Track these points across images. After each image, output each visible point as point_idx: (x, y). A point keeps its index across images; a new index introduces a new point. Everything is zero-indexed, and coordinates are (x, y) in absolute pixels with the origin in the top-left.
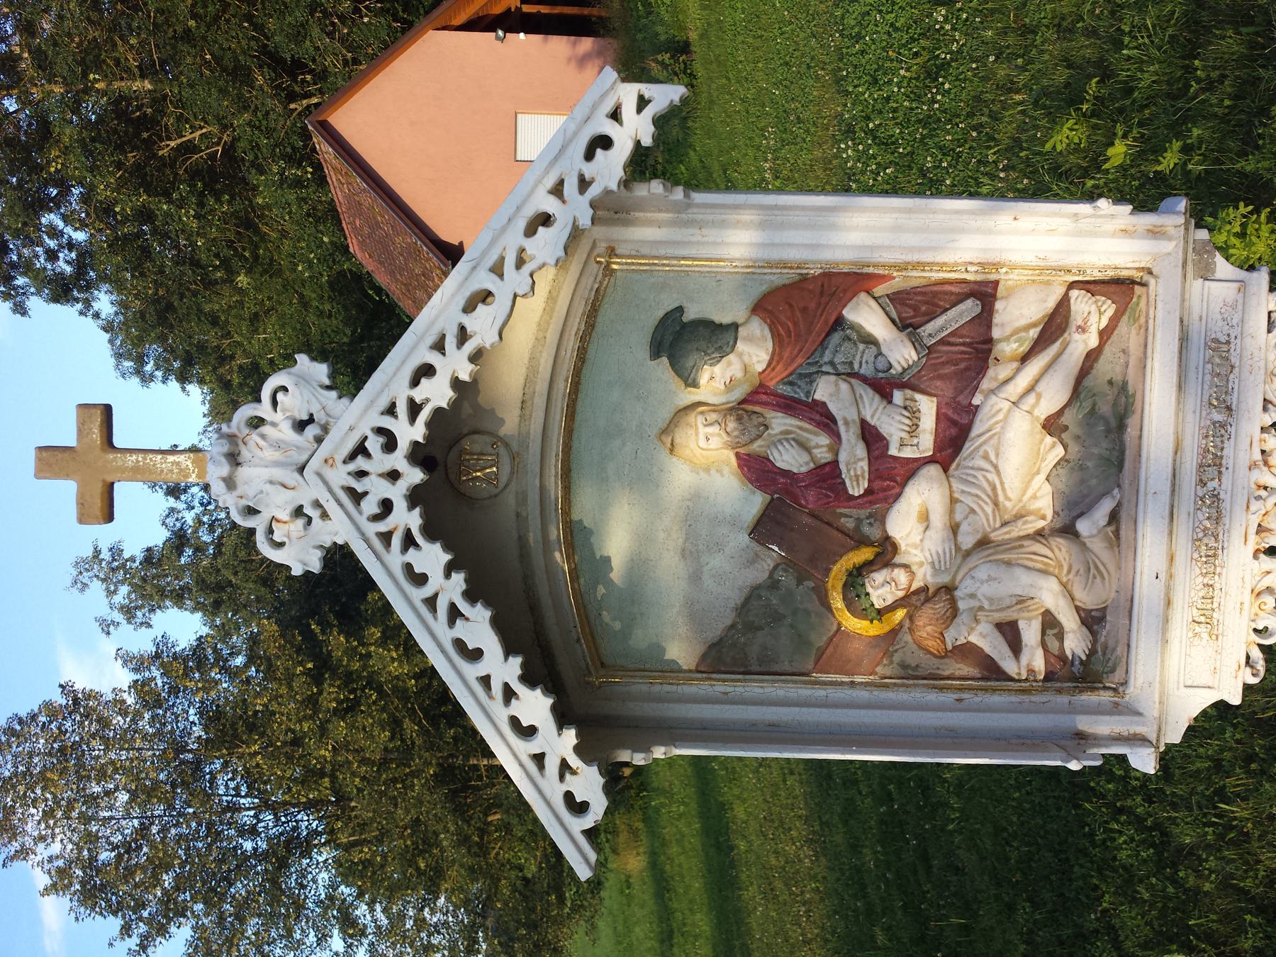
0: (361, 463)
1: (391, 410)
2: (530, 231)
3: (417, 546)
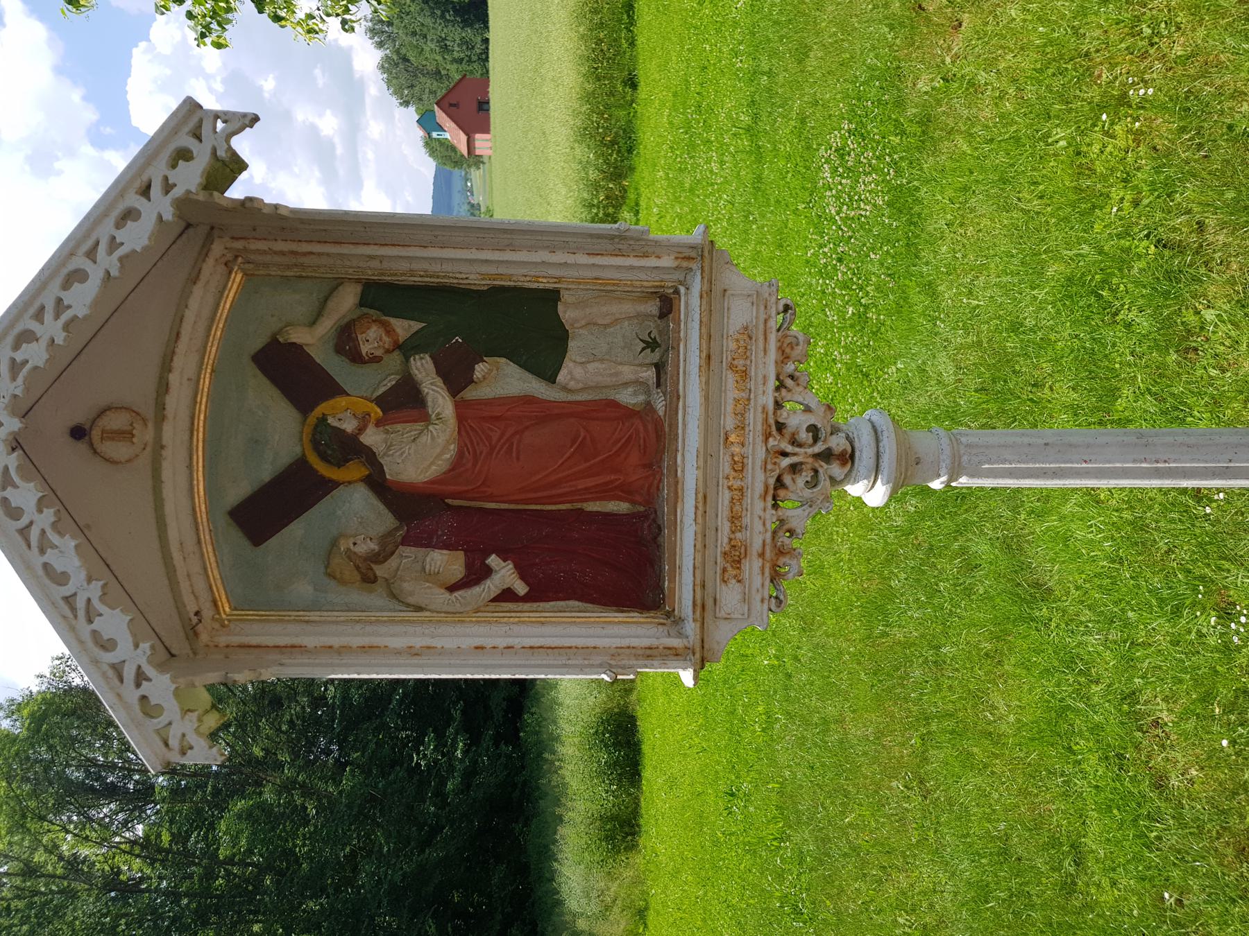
3: (15, 486)
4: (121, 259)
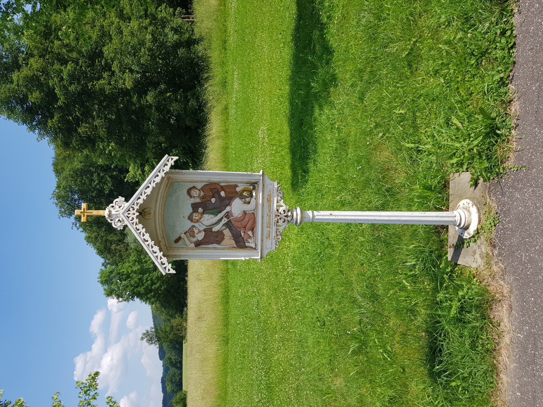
0: (129, 212)
1: (134, 204)
2: (155, 178)
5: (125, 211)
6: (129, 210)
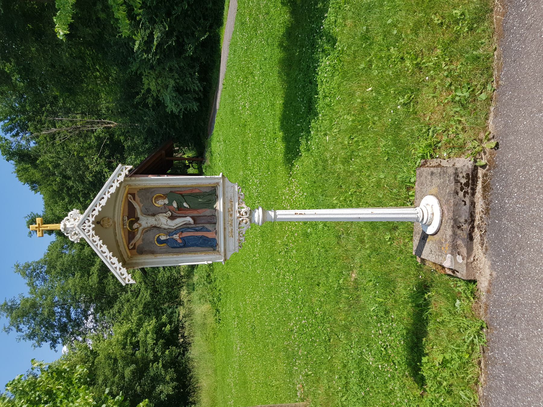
0: (84, 224)
1: (89, 216)
4: (110, 194)
5: (80, 224)
6: (85, 223)
